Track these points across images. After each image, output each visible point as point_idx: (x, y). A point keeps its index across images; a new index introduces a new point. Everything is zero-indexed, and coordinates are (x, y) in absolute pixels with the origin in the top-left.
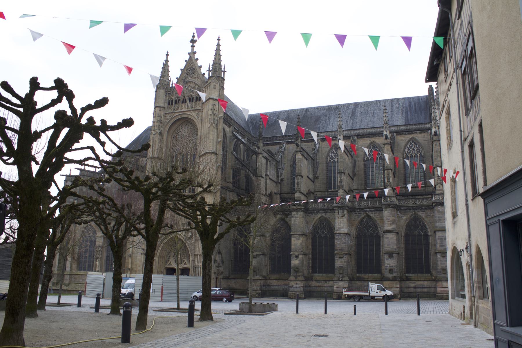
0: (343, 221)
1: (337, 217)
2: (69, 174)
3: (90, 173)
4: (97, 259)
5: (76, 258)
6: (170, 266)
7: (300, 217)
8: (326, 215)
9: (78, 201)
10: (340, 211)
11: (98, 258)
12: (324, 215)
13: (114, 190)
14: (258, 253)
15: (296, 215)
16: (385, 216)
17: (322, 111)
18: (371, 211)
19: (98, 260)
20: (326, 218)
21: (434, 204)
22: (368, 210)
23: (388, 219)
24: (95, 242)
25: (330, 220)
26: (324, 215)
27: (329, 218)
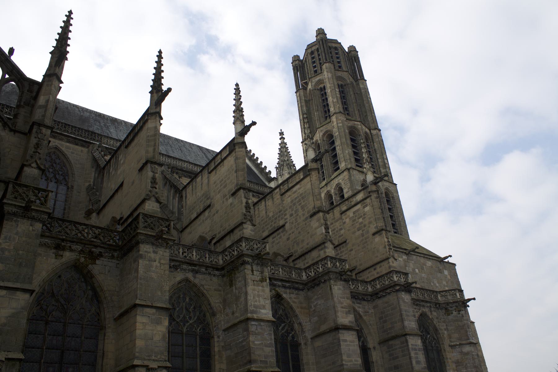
0: (263, 291)
1: (249, 280)
7: (162, 261)
8: (195, 277)
10: (255, 267)
12: (190, 276)
14: (11, 355)
15: (152, 255)
16: (336, 295)
17: (88, 114)
18: (284, 287)
20: (195, 285)
21: (398, 288)
22: (280, 283)
23: (342, 303)
25: (205, 291)
26: (190, 276)
27: (203, 286)
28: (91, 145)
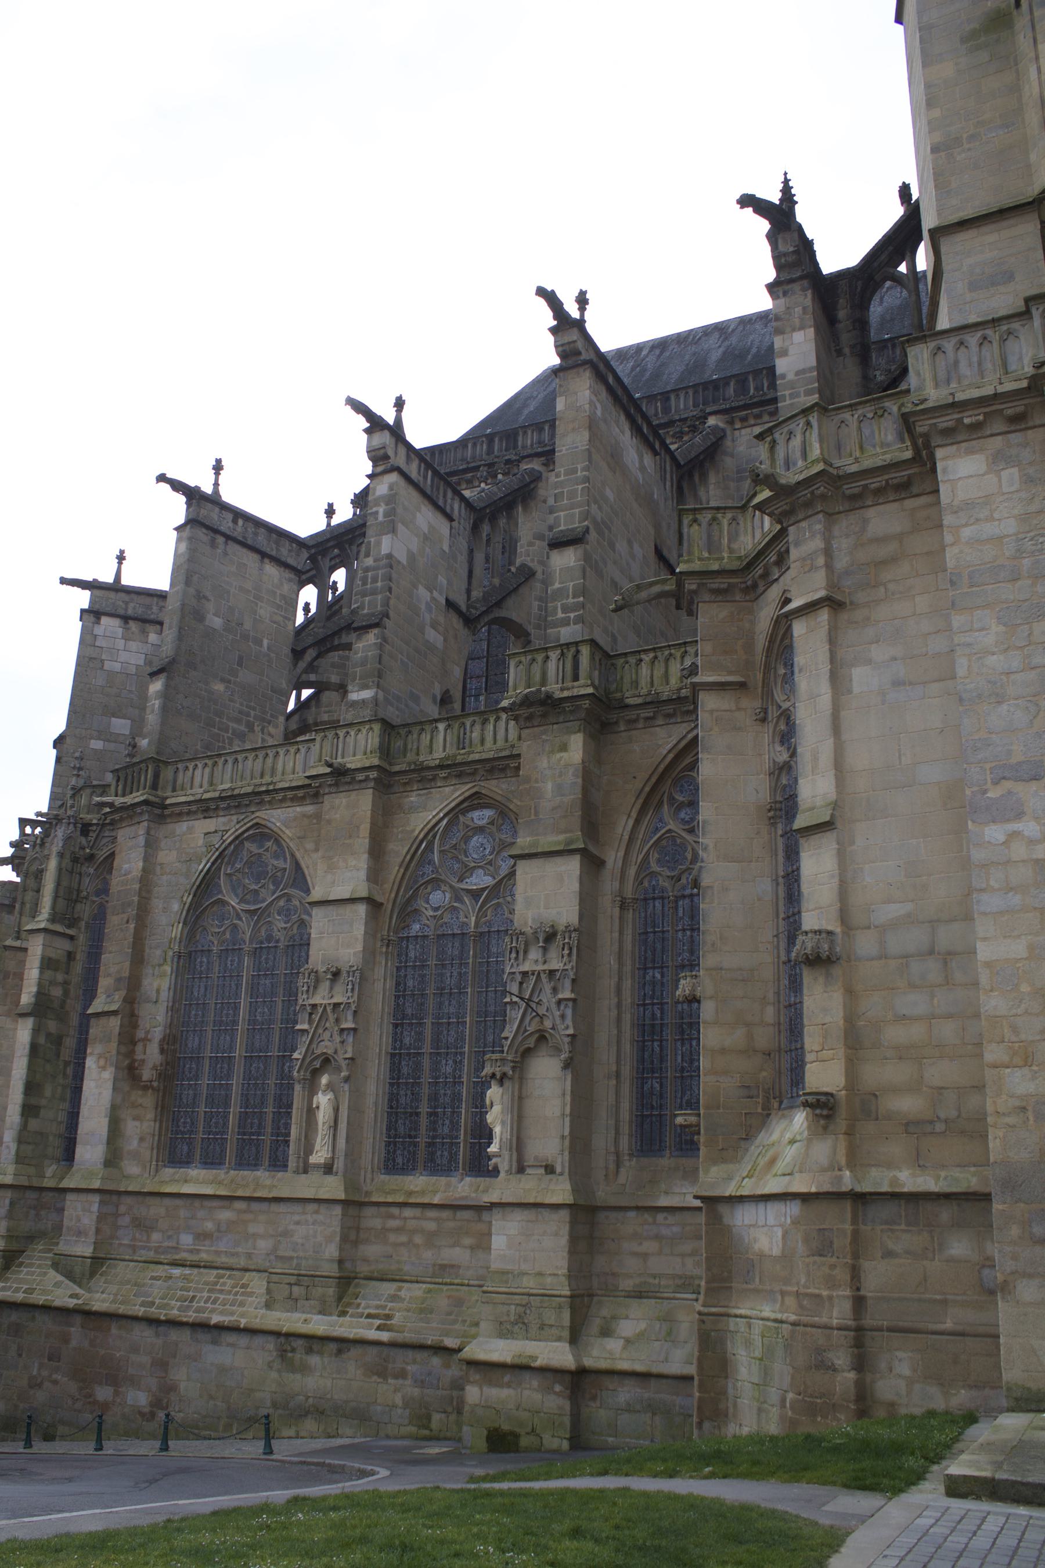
2: (109, 578)
3: (251, 529)
4: (316, 1073)
5: (147, 1074)
9: (169, 679)
11: (327, 1061)
13: (422, 592)
19: (324, 1080)
24: (301, 944)
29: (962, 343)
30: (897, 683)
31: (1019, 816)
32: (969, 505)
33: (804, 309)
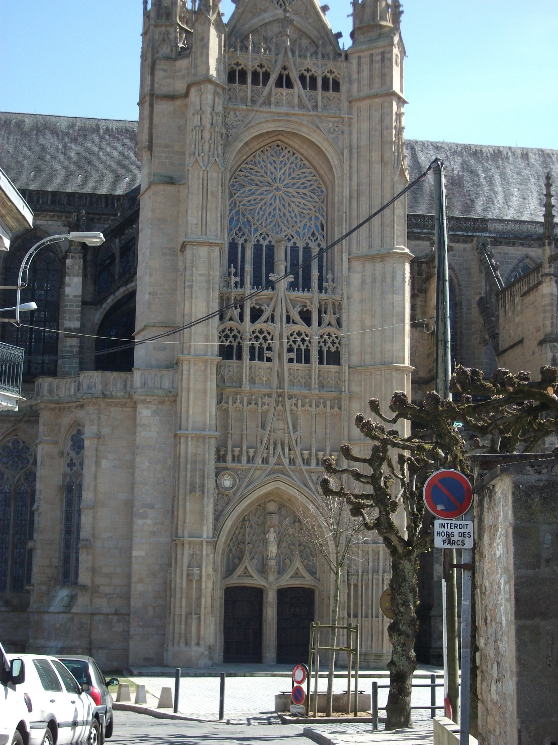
6: (248, 582)
28: (476, 239)
29: (150, 373)
30: (114, 467)
31: (146, 518)
32: (144, 425)
33: (79, 267)
